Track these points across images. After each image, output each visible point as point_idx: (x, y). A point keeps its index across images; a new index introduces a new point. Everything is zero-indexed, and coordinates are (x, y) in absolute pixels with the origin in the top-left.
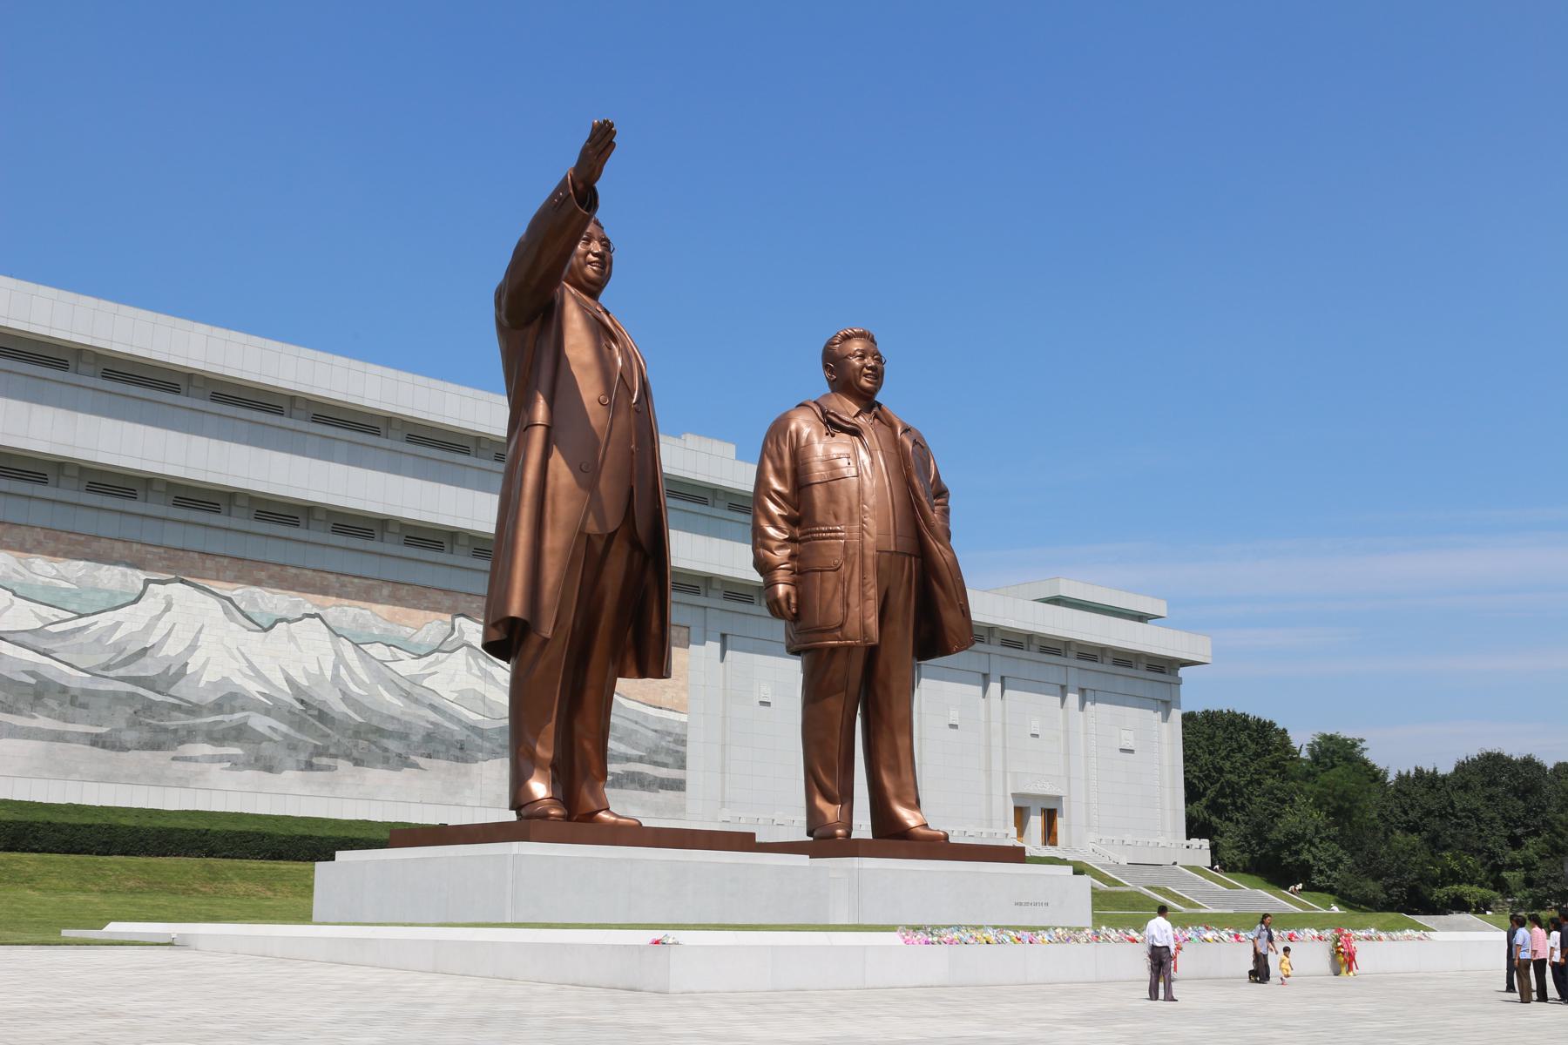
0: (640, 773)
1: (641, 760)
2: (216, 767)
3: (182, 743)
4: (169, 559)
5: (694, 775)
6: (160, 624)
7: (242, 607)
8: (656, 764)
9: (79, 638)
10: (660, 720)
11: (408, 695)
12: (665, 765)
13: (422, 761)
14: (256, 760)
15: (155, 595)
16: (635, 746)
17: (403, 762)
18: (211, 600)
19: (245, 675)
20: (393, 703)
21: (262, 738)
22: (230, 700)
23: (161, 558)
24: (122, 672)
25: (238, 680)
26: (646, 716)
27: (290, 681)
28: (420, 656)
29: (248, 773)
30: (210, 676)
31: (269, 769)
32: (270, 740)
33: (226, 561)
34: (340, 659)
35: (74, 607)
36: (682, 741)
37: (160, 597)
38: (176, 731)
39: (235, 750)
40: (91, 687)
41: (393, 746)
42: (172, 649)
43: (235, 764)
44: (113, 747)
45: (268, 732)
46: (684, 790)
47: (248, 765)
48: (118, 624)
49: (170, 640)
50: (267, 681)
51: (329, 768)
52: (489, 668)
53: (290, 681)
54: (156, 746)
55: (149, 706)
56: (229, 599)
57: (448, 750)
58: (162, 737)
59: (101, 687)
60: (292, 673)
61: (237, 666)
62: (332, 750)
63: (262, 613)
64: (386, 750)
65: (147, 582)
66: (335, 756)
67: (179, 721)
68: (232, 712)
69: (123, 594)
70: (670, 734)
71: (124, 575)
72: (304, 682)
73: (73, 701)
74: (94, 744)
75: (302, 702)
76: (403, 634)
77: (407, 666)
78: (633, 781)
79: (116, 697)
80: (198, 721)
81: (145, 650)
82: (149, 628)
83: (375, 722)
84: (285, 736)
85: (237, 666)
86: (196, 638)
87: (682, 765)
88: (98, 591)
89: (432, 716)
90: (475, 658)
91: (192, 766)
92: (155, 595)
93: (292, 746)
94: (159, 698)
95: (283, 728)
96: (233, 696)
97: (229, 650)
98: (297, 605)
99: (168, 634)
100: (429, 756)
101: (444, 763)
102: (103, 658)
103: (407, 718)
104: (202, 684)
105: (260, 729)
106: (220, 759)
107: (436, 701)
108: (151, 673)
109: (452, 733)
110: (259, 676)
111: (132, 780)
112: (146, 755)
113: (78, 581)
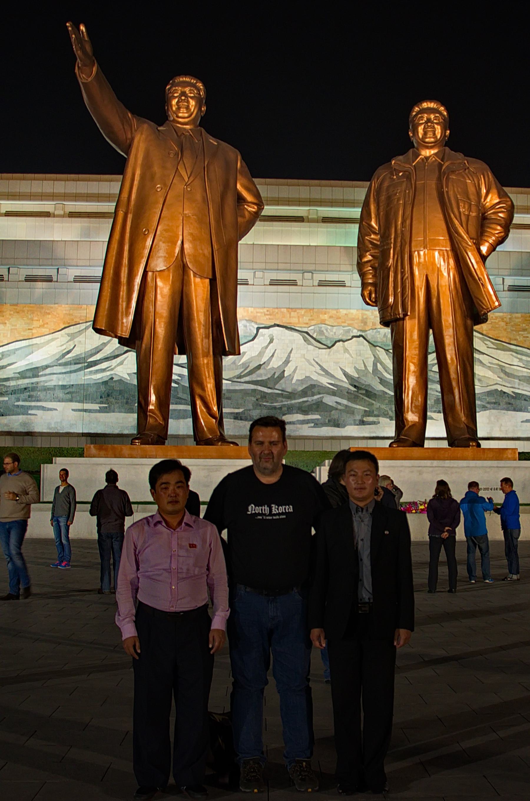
2: (306, 426)
4: (270, 315)
6: (268, 351)
7: (314, 336)
14: (329, 421)
15: (263, 335)
19: (319, 374)
21: (332, 408)
22: (312, 388)
23: (265, 315)
24: (247, 379)
25: (315, 377)
27: (346, 374)
31: (338, 425)
32: (337, 409)
34: (377, 360)
37: (266, 336)
38: (281, 408)
39: (318, 417)
40: (232, 388)
42: (275, 363)
43: (317, 424)
45: (334, 405)
47: (324, 425)
49: (274, 359)
50: (332, 376)
51: (373, 423)
53: (346, 374)
55: (264, 396)
56: (307, 333)
61: (314, 369)
62: (375, 413)
63: (327, 338)
65: (258, 329)
66: (378, 416)
68: (313, 396)
69: (244, 336)
71: (245, 326)
74: (236, 418)
75: (355, 386)
79: (245, 392)
80: (293, 402)
81: (260, 365)
82: (261, 354)
85: (314, 369)
86: (289, 356)
92: (263, 335)
94: (270, 391)
95: (345, 402)
96: (313, 386)
97: (308, 361)
98: (348, 331)
99: (273, 356)
102: (237, 372)
104: (294, 381)
105: (330, 404)
108: (264, 378)
110: (327, 373)
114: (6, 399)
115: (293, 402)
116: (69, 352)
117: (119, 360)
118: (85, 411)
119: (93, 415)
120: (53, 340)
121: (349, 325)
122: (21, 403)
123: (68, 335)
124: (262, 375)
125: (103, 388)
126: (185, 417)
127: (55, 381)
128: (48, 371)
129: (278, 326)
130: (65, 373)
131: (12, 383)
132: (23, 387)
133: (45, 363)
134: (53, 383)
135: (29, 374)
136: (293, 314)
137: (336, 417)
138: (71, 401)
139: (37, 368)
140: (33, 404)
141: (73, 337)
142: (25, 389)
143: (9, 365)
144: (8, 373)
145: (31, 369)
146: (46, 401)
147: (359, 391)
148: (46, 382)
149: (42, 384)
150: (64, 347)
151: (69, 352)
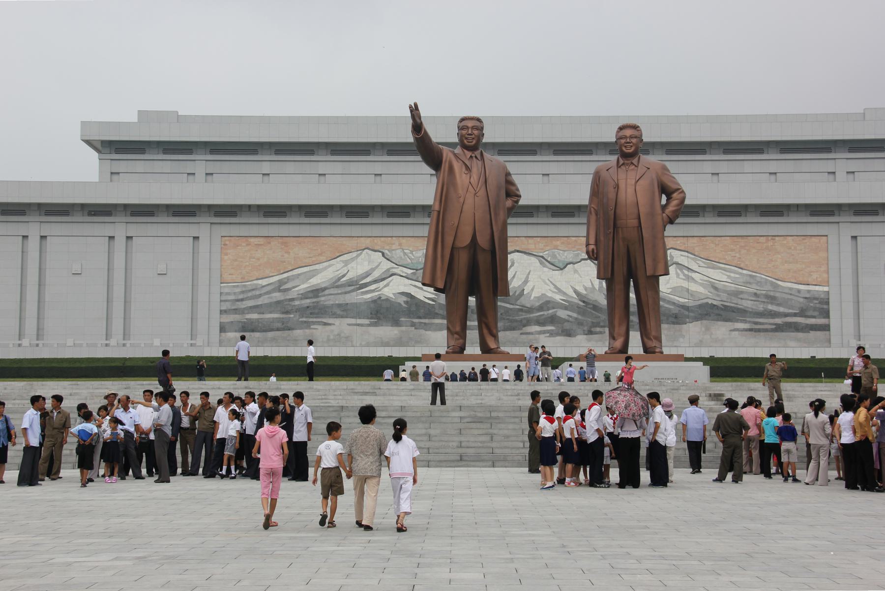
0: (795, 323)
1: (795, 315)
2: (542, 336)
3: (524, 326)
5: (834, 321)
10: (809, 291)
12: (814, 317)
16: (791, 307)
18: (533, 259)
22: (547, 304)
25: (549, 294)
26: (799, 291)
27: (576, 292)
29: (559, 338)
32: (569, 321)
33: (539, 239)
36: (828, 303)
43: (552, 334)
45: (567, 318)
46: (829, 330)
47: (558, 334)
50: (565, 294)
52: (690, 274)
53: (576, 292)
54: (513, 329)
56: (542, 257)
58: (515, 324)
60: (577, 288)
62: (602, 324)
63: (559, 261)
67: (524, 316)
70: (816, 299)
72: (584, 292)
75: (584, 302)
80: (532, 315)
84: (576, 319)
86: (527, 277)
87: (826, 314)
91: (531, 337)
93: (580, 324)
94: (512, 307)
95: (575, 315)
96: (548, 302)
98: (578, 255)
104: (532, 298)
109: (669, 309)
110: (560, 291)
115: (532, 315)
116: (344, 276)
117: (385, 282)
118: (358, 325)
120: (330, 266)
121: (578, 250)
122: (304, 319)
123: (343, 261)
126: (441, 330)
128: (327, 292)
129: (518, 251)
133: (323, 286)
134: (332, 303)
135: (310, 295)
136: (531, 241)
137: (568, 328)
138: (347, 317)
139: (317, 290)
140: (315, 320)
141: (346, 263)
144: (293, 294)
145: (312, 291)
147: (586, 305)
148: (324, 301)
151: (344, 276)
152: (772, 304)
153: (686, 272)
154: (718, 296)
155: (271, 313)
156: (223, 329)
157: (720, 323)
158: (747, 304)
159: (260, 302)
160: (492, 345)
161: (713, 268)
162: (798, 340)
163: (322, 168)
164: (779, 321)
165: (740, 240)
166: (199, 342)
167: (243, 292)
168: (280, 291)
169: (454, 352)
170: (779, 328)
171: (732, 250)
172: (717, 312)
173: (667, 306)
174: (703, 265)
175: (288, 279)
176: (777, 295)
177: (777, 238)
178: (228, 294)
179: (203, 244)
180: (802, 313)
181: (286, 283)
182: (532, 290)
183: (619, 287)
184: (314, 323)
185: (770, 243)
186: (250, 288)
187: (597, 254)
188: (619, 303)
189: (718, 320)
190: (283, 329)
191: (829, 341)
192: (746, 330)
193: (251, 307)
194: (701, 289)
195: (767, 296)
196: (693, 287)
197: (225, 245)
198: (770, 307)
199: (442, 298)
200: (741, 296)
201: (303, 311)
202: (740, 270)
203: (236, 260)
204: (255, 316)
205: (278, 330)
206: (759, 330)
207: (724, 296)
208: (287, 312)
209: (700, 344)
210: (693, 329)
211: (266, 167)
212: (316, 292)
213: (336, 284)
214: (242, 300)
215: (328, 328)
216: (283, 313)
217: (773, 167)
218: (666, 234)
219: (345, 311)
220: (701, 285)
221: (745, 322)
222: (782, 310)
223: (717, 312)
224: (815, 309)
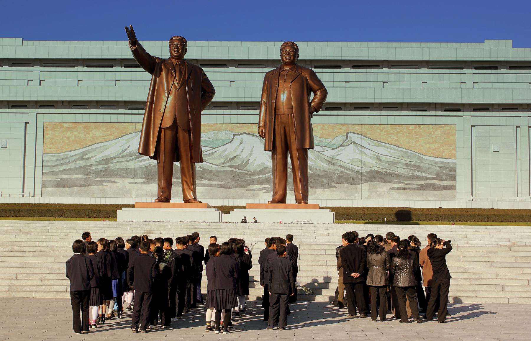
1: (434, 179)
2: (261, 192)
3: (249, 185)
4: (241, 127)
8: (441, 180)
9: (215, 155)
10: (442, 163)
11: (329, 162)
13: (337, 185)
17: (330, 186)
20: (326, 166)
24: (228, 164)
26: (436, 163)
28: (334, 149)
30: (257, 163)
35: (212, 146)
36: (454, 171)
39: (268, 186)
40: (219, 170)
41: (324, 180)
42: (244, 156)
43: (267, 190)
44: (227, 188)
46: (455, 189)
48: (226, 150)
54: (242, 187)
55: (237, 174)
57: (347, 181)
59: (222, 170)
64: (322, 182)
65: (234, 135)
67: (248, 178)
73: (214, 174)
74: (221, 187)
76: (327, 141)
77: (330, 153)
78: (430, 187)
81: (235, 156)
82: (235, 150)
83: (318, 173)
86: (252, 151)
87: (454, 179)
88: (218, 140)
89: (340, 169)
90: (356, 147)
91: (253, 192)
99: (242, 151)
100: (340, 183)
101: (346, 185)
103: (330, 171)
104: (254, 166)
106: (262, 189)
107: (342, 164)
109: (349, 174)
111: (234, 197)
112: (238, 189)
113: (212, 138)
114: (91, 176)
116: (126, 149)
118: (136, 183)
119: (140, 185)
122: (99, 179)
124: (237, 162)
125: (145, 170)
127: (118, 166)
128: (115, 160)
129: (246, 133)
130: (124, 162)
131: (94, 168)
132: (100, 170)
133: (112, 156)
135: (103, 162)
139: (108, 159)
140: (106, 179)
142: (101, 171)
143: (92, 157)
144: (92, 162)
145: (105, 160)
146: (113, 178)
149: (111, 168)
150: (123, 147)
151: (126, 149)
152: (418, 171)
153: (360, 149)
154: (382, 165)
155: (76, 174)
156: (43, 185)
157: (382, 184)
158: (402, 171)
159: (68, 167)
160: (190, 195)
161: (379, 146)
162: (435, 196)
163: (118, 76)
164: (422, 183)
165: (397, 127)
166: (26, 193)
167: (57, 160)
168: (83, 159)
169: (160, 201)
170: (422, 188)
171: (392, 134)
172: (380, 176)
173: (346, 171)
174: (372, 144)
175: (88, 152)
176: (422, 165)
177: (422, 126)
178: (47, 161)
179: (31, 129)
180: (439, 177)
181: (87, 154)
182: (255, 160)
183: (279, 157)
184: (106, 182)
185: (418, 130)
186: (63, 157)
187: (265, 133)
188: (280, 167)
189: (381, 182)
190: (85, 186)
191: (455, 197)
192: (400, 189)
193: (63, 170)
194: (370, 161)
195: (415, 166)
196: (366, 159)
197: (47, 128)
198: (417, 173)
199: (155, 162)
200: (397, 166)
201: (97, 173)
202: (397, 148)
203: (54, 138)
204: (65, 176)
205: (81, 186)
206: (409, 189)
207: (386, 166)
208: (87, 174)
209: (368, 199)
210: (364, 188)
211: (80, 76)
212: (107, 160)
213: (120, 156)
214: (57, 165)
215: (115, 185)
216: (85, 174)
217: (424, 78)
218: (313, 120)
219: (127, 173)
220: (370, 157)
221: (399, 183)
222: (424, 175)
223: (380, 176)
224: (446, 175)
